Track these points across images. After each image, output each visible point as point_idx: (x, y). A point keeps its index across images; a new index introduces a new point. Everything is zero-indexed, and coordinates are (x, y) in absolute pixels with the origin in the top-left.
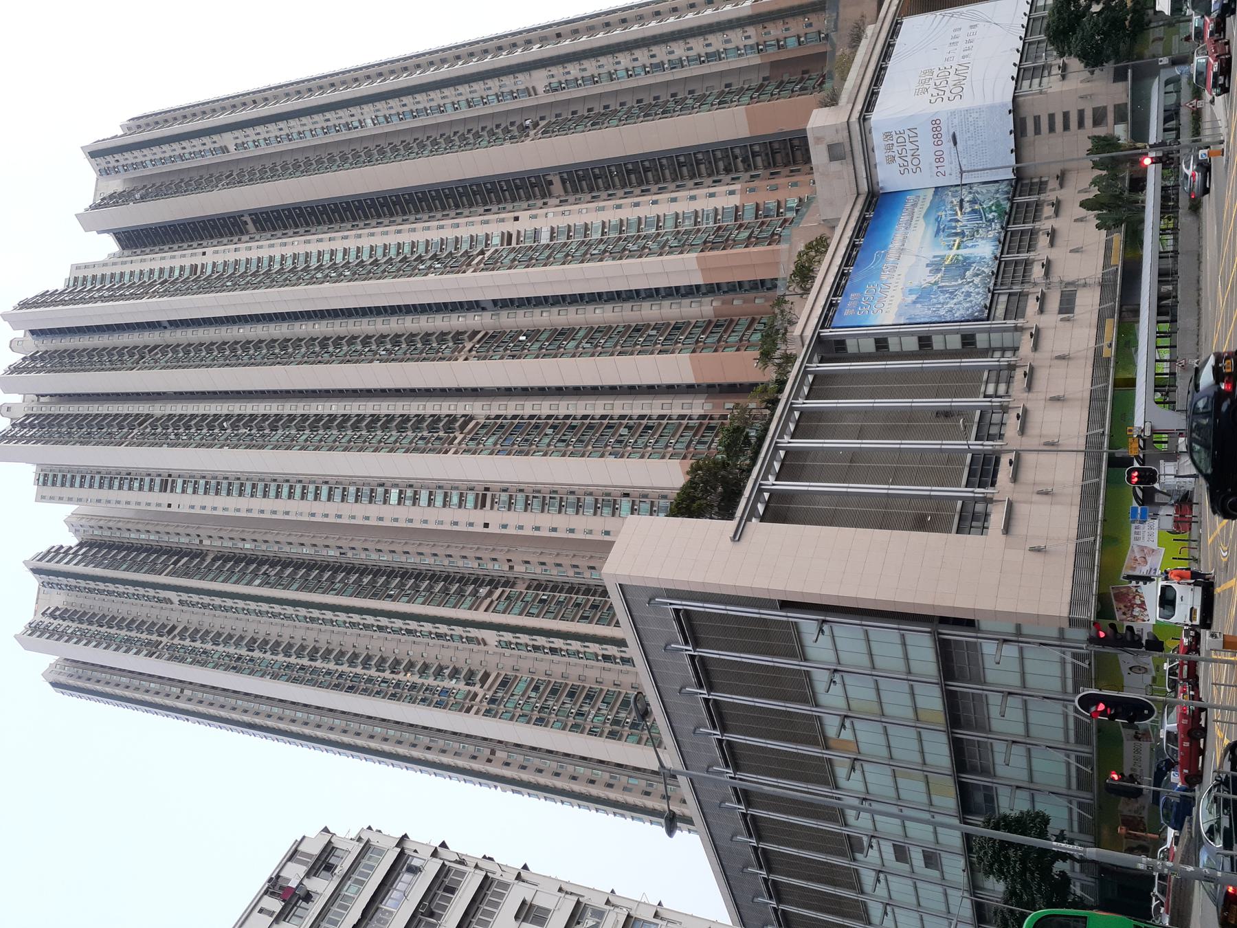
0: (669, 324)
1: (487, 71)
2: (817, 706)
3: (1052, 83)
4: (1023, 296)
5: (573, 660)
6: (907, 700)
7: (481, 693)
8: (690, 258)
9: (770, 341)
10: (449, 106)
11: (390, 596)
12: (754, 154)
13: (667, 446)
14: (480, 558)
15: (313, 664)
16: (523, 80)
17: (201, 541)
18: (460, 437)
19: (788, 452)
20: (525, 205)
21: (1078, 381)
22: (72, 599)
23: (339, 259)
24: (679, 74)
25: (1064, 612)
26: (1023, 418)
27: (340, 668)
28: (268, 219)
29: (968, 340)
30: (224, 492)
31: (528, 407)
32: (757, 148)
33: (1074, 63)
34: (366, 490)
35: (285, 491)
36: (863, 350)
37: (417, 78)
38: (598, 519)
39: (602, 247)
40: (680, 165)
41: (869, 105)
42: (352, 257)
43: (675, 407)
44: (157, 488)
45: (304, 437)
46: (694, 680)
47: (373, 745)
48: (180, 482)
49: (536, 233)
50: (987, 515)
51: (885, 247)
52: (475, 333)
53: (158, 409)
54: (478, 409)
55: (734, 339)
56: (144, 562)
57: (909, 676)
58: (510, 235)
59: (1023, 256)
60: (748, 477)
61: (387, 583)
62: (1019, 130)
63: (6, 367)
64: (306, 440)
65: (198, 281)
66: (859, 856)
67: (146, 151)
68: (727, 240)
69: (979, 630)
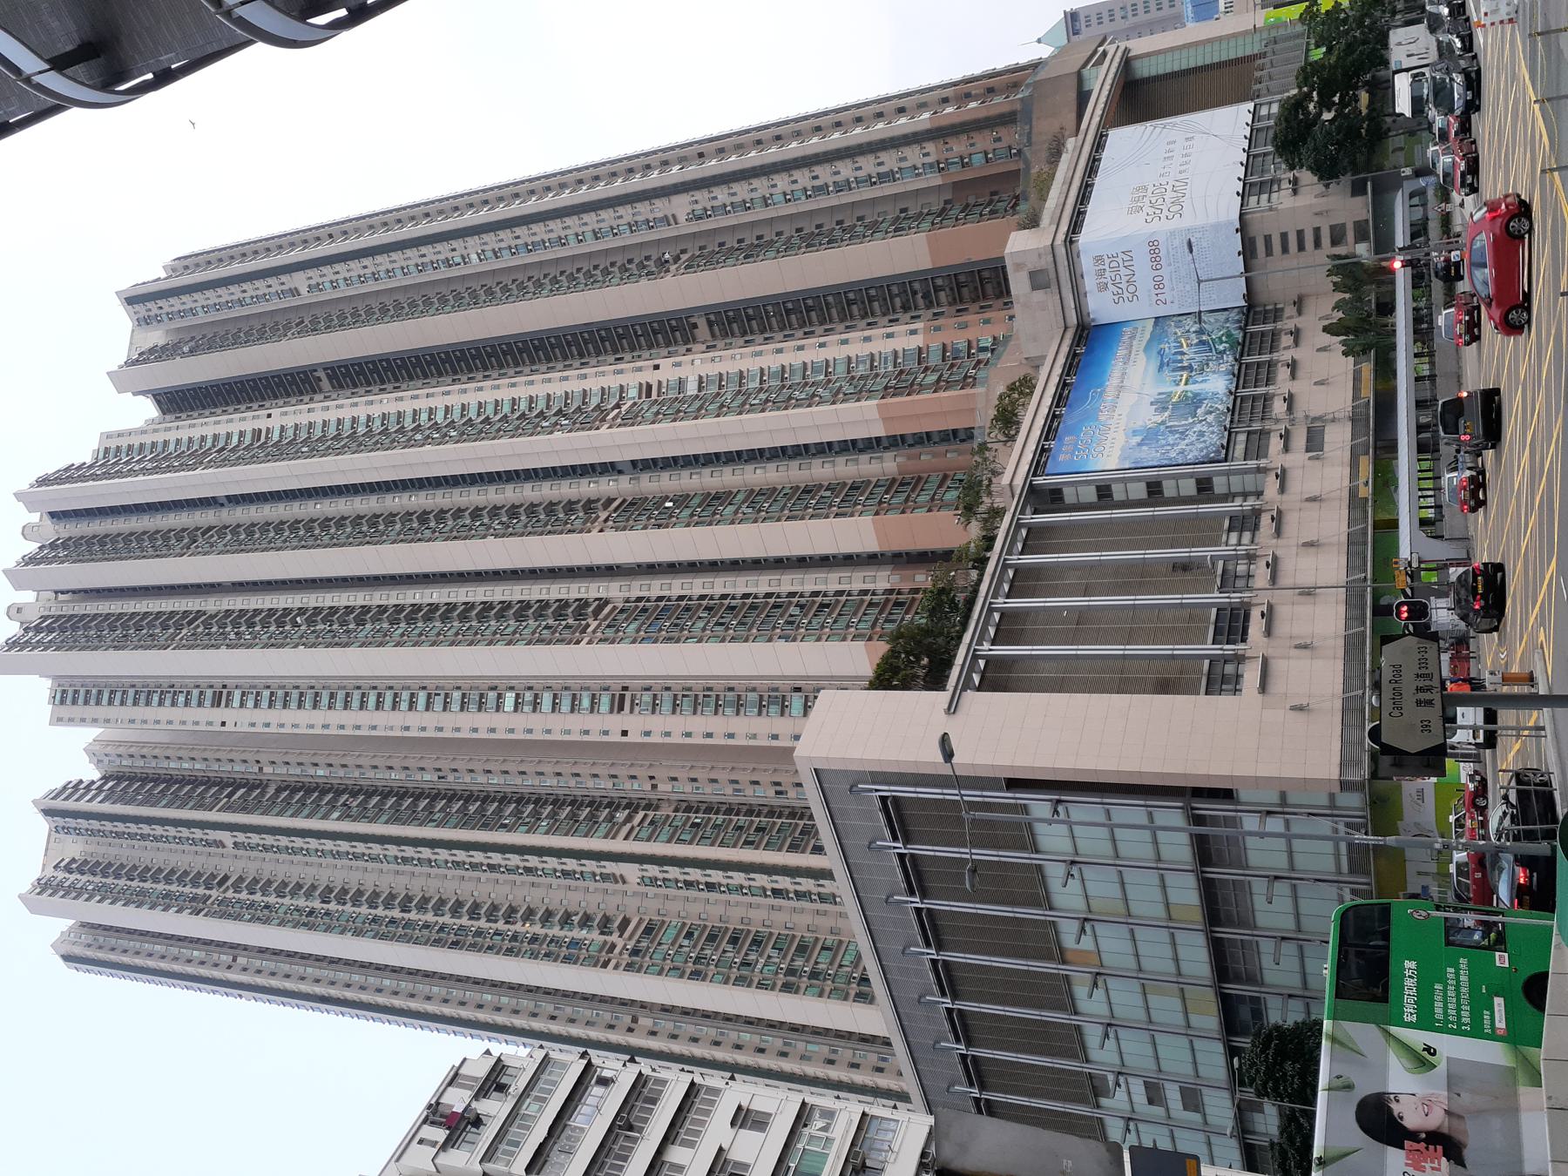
0: (845, 484)
1: (654, 189)
2: (1051, 909)
3: (1283, 199)
4: (1264, 434)
5: (735, 897)
6: (1157, 894)
7: (620, 943)
8: (870, 406)
9: (972, 496)
10: (572, 239)
11: (504, 826)
12: (937, 289)
13: (848, 627)
14: (615, 776)
15: (406, 915)
16: (661, 207)
17: (261, 769)
18: (594, 624)
19: (1004, 614)
20: (664, 352)
21: (1334, 523)
22: (91, 848)
23: (440, 418)
24: (846, 198)
25: (1335, 774)
26: (1274, 566)
27: (441, 920)
28: (347, 374)
29: (1204, 487)
30: (294, 705)
31: (676, 587)
32: (939, 282)
33: (1306, 176)
34: (475, 696)
35: (372, 699)
36: (1083, 500)
37: (532, 205)
38: (763, 720)
39: (763, 396)
40: (850, 303)
41: (1076, 225)
42: (456, 415)
43: (857, 581)
44: (208, 703)
45: (400, 631)
46: (903, 885)
47: (482, 1016)
48: (237, 695)
49: (681, 383)
50: (1238, 677)
51: (1101, 385)
52: (610, 501)
53: (212, 604)
54: (614, 590)
55: (923, 498)
56: (189, 795)
57: (1159, 864)
58: (649, 387)
59: (1261, 390)
60: (958, 646)
61: (499, 811)
62: (1248, 251)
63: (19, 557)
64: (402, 635)
65: (261, 448)
66: (1104, 1101)
67: (196, 296)
68: (912, 384)
69: (1238, 803)
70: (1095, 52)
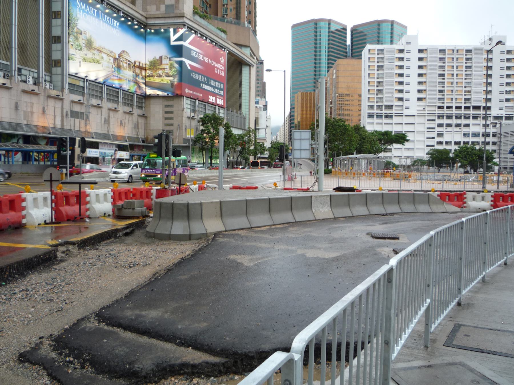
70: (255, 55)
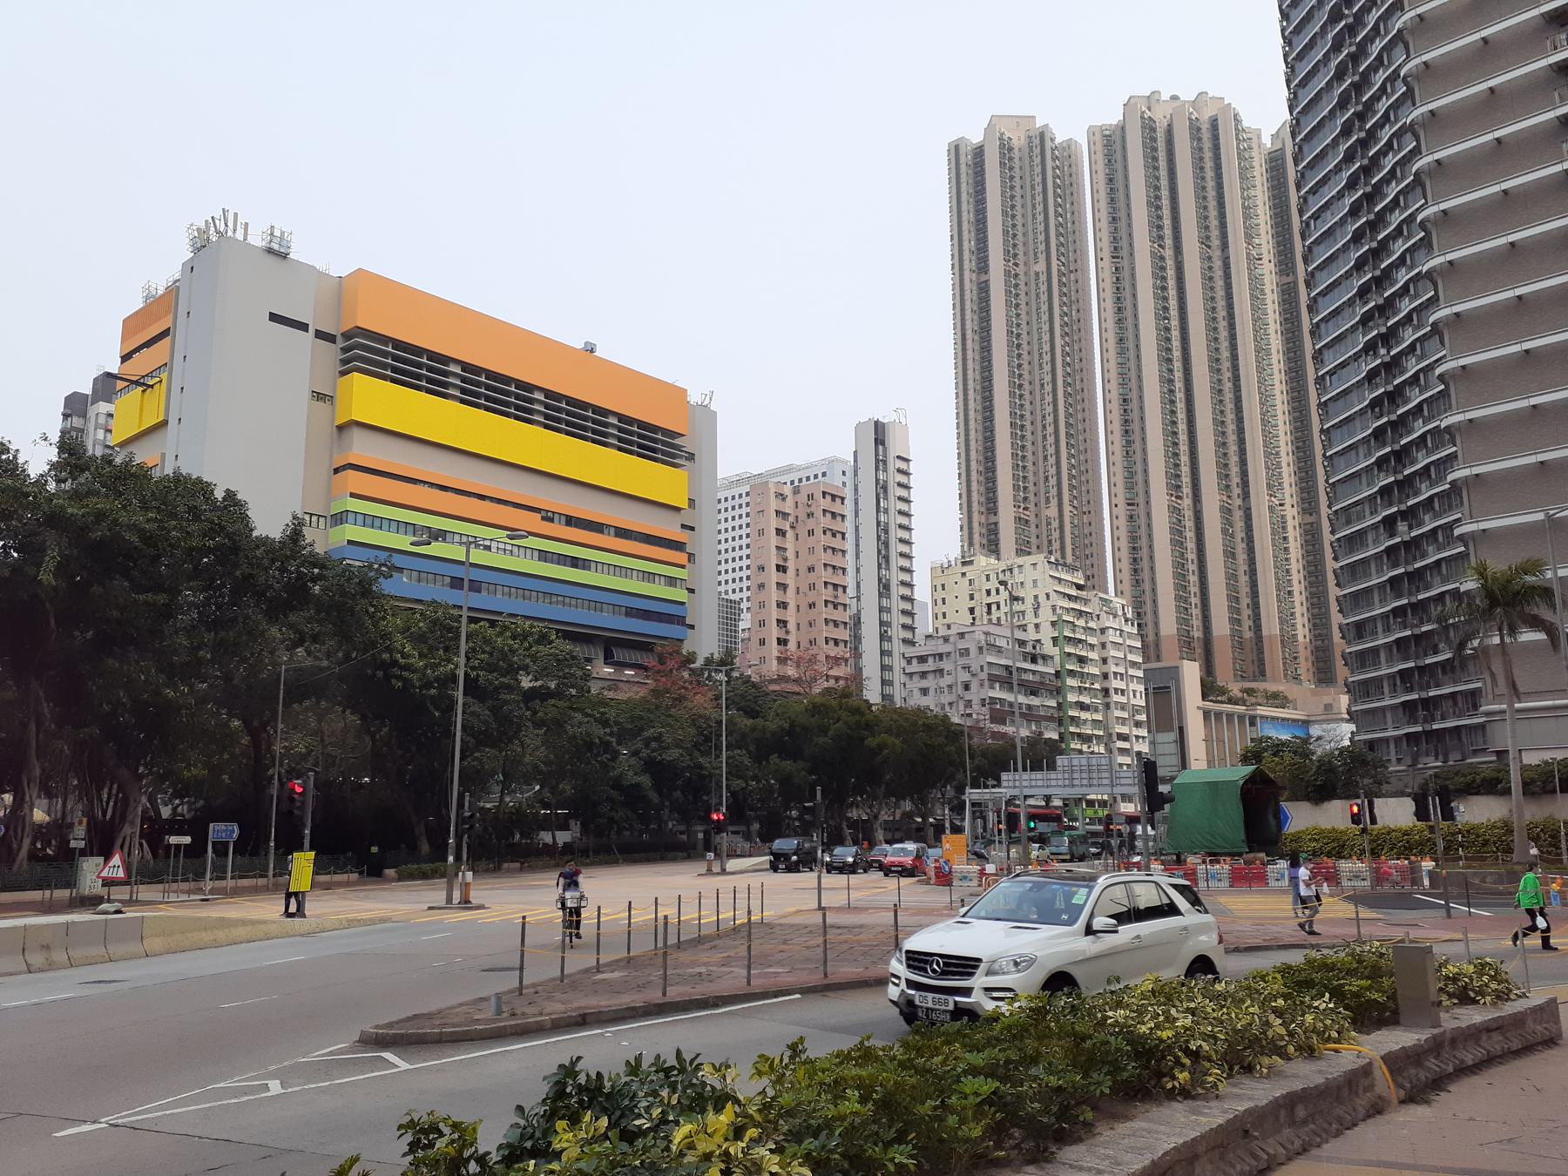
54: (1187, 502)
